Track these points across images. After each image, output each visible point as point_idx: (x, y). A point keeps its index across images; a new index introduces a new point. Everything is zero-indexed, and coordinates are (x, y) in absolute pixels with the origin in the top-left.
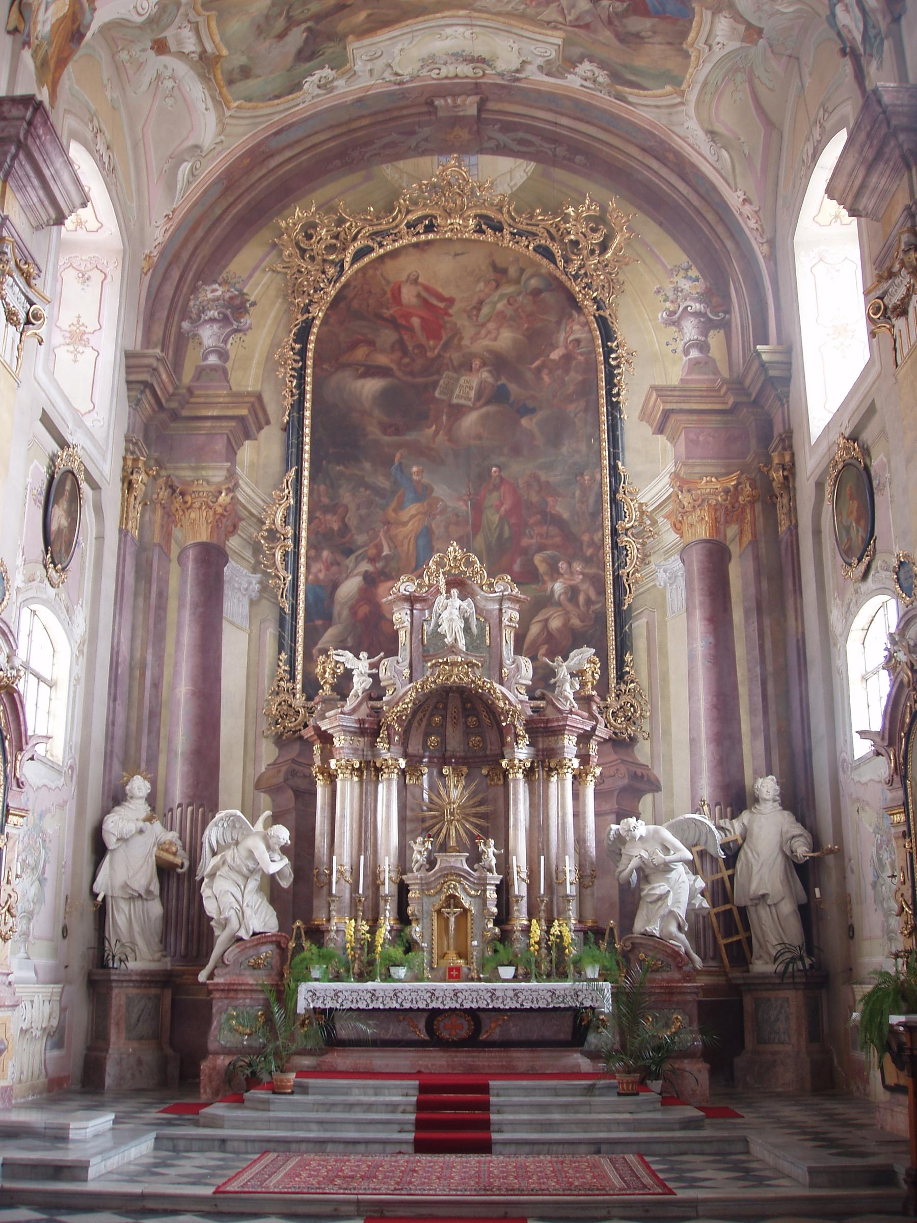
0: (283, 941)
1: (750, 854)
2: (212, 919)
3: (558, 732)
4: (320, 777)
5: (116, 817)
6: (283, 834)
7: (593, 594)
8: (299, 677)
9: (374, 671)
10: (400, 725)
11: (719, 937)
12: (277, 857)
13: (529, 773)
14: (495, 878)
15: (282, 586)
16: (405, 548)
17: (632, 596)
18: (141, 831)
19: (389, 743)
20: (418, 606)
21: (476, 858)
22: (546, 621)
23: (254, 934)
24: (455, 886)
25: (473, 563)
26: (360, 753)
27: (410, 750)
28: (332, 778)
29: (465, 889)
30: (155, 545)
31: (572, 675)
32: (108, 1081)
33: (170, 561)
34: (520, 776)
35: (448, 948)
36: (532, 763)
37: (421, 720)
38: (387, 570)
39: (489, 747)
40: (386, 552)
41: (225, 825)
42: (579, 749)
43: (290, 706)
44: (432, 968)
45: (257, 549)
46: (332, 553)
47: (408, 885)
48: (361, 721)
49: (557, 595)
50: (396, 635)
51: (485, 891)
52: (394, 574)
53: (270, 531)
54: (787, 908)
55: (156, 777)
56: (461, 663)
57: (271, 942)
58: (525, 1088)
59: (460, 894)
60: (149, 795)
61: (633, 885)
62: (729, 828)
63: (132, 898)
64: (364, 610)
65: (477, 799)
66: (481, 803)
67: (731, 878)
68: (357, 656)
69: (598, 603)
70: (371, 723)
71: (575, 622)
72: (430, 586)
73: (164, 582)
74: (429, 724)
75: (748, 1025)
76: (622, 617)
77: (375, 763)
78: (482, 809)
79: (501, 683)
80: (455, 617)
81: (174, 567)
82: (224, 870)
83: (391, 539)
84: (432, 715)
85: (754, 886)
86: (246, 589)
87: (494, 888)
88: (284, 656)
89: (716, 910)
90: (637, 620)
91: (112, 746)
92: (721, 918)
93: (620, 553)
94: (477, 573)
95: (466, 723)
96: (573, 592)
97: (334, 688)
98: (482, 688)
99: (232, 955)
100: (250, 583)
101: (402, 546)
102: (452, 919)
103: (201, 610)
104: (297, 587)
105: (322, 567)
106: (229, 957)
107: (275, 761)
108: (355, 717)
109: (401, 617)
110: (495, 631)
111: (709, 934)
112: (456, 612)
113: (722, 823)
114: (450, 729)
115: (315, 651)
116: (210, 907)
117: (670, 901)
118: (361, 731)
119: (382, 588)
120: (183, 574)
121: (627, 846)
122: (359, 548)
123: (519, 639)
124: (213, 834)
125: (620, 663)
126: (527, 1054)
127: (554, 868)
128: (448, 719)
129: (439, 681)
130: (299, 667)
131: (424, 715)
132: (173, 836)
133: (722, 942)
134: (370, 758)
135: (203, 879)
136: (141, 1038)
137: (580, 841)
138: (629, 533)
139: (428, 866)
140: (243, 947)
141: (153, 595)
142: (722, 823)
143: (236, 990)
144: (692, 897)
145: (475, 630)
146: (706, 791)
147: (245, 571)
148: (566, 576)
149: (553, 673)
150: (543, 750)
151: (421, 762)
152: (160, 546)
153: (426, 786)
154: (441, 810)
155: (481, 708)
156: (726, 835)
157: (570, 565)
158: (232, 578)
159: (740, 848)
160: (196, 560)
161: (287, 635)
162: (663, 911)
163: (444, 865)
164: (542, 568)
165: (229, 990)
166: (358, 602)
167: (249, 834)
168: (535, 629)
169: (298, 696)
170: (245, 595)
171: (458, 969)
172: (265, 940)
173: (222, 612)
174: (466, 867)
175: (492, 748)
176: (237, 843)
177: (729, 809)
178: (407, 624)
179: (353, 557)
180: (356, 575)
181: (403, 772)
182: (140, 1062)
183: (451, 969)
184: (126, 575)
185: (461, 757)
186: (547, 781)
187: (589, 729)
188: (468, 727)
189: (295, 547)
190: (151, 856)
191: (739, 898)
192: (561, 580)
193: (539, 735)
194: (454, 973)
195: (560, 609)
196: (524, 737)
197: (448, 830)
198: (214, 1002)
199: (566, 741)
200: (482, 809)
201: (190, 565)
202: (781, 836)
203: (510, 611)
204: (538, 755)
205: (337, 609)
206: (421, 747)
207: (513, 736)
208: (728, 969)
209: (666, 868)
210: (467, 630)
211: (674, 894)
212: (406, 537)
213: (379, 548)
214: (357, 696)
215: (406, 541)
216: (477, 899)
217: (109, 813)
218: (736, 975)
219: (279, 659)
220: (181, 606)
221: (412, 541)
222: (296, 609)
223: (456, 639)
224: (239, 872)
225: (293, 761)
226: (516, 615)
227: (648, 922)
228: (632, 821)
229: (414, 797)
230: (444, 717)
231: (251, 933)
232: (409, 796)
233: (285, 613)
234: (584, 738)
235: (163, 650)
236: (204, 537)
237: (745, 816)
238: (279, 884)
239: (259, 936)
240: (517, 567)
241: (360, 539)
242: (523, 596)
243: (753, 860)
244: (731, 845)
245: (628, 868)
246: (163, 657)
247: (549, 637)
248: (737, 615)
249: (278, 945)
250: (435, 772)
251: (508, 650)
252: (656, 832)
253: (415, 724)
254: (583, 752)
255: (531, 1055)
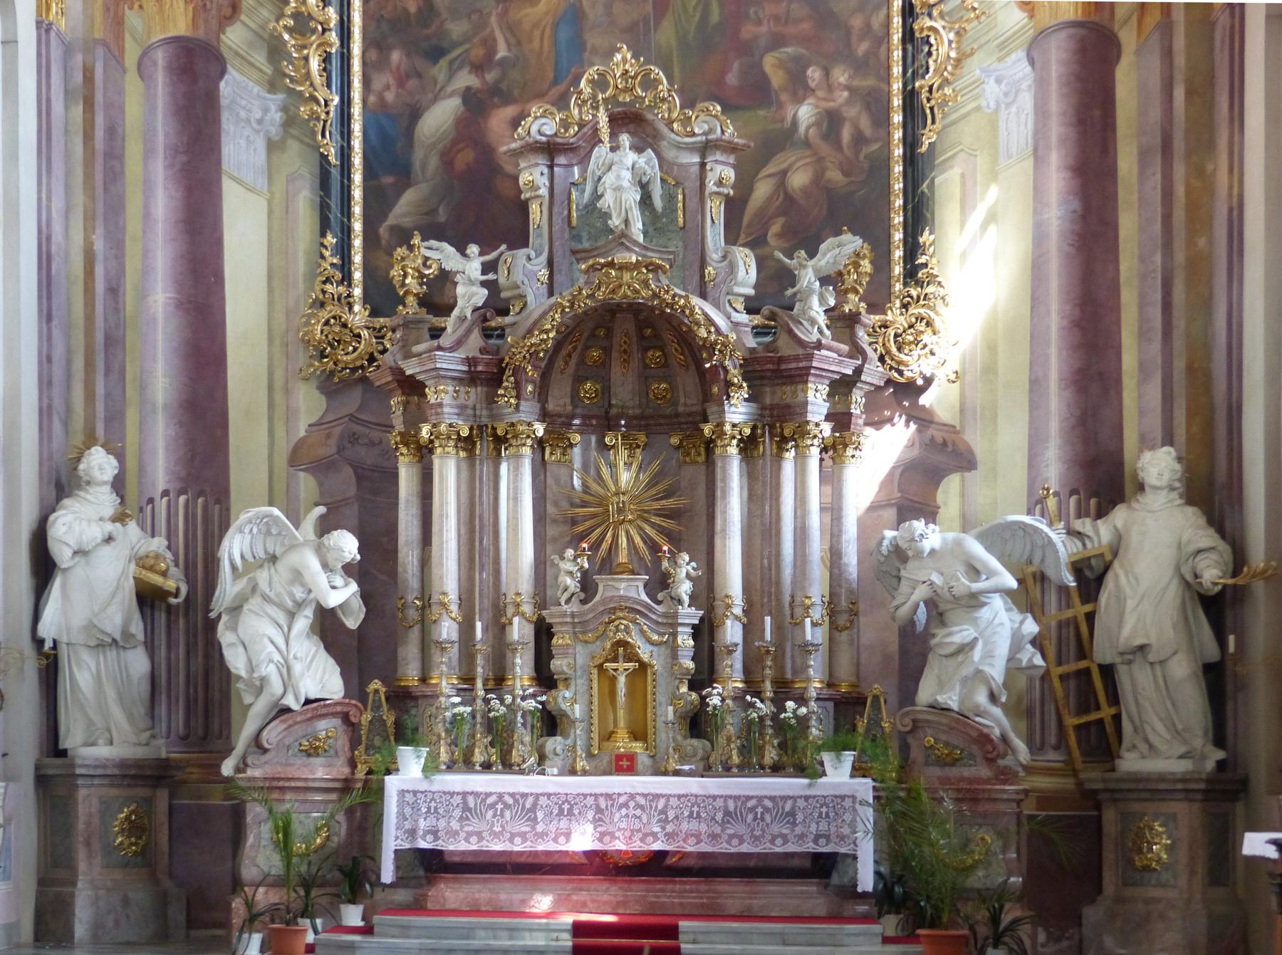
0: (352, 712)
1: (1123, 579)
2: (239, 678)
3: (800, 377)
4: (404, 450)
5: (70, 517)
6: (347, 545)
7: (865, 124)
8: (357, 275)
9: (491, 276)
10: (535, 368)
11: (1064, 713)
12: (339, 581)
13: (748, 446)
14: (690, 615)
15: (323, 116)
16: (536, 44)
17: (938, 126)
18: (109, 539)
19: (518, 397)
20: (561, 160)
21: (660, 583)
22: (783, 174)
23: (308, 702)
24: (627, 627)
25: (657, 82)
26: (470, 412)
27: (551, 406)
28: (424, 453)
29: (642, 632)
30: (96, 42)
31: (824, 281)
32: (81, 930)
33: (125, 72)
34: (733, 450)
35: (616, 725)
36: (754, 428)
37: (570, 355)
38: (504, 86)
39: (682, 400)
40: (502, 52)
41: (255, 530)
42: (833, 405)
43: (345, 325)
44: (590, 756)
45: (276, 51)
46: (408, 55)
47: (550, 626)
48: (470, 361)
49: (802, 129)
50: (524, 208)
51: (674, 635)
52: (516, 92)
53: (296, 15)
54: (1182, 669)
55: (123, 448)
56: (637, 265)
57: (334, 715)
58: (736, 933)
59: (636, 639)
60: (116, 477)
61: (920, 627)
62: (1091, 534)
63: (100, 646)
64: (465, 158)
65: (660, 487)
66: (668, 494)
67: (1090, 617)
68: (462, 251)
69: (877, 140)
70: (487, 364)
71: (834, 175)
72: (581, 125)
73: (116, 110)
74: (581, 362)
75: (1109, 856)
76: (917, 166)
77: (494, 429)
78: (669, 503)
79: (703, 296)
80: (626, 184)
81: (132, 84)
82: (254, 603)
83: (512, 29)
84: (587, 348)
85: (1126, 631)
86: (260, 122)
87: (689, 630)
88: (330, 240)
89: (1061, 670)
90: (945, 171)
91: (50, 398)
92: (1072, 684)
93: (916, 51)
94: (663, 100)
95: (643, 360)
96: (831, 121)
97: (424, 302)
98: (671, 306)
99: (274, 734)
100: (266, 111)
101: (530, 41)
102: (622, 680)
103: (184, 158)
104: (349, 116)
105: (392, 81)
106: (272, 735)
107: (322, 418)
108: (461, 354)
109: (533, 176)
110: (693, 204)
111: (1051, 709)
112: (627, 175)
113: (1078, 525)
114: (617, 371)
115: (383, 231)
116: (236, 661)
117: (977, 654)
118: (471, 378)
119: (499, 119)
120: (149, 98)
121: (910, 565)
122: (455, 45)
123: (734, 207)
124: (234, 546)
125: (912, 249)
126: (741, 888)
127: (787, 599)
128: (614, 354)
129: (600, 295)
130: (357, 259)
131: (575, 348)
132: (158, 544)
133: (1071, 721)
134: (485, 420)
135: (219, 616)
136: (126, 865)
137: (835, 556)
138: (935, 13)
139: (582, 596)
140: (291, 722)
141: (99, 134)
142: (1078, 525)
143: (282, 789)
144: (1016, 647)
145: (658, 203)
146: (1054, 471)
147: (256, 89)
148: (820, 93)
149: (789, 278)
150: (772, 407)
151: (569, 425)
152: (104, 43)
153: (577, 464)
154: (602, 502)
155: (668, 337)
156: (1084, 545)
157: (827, 73)
158: (233, 101)
159: (1107, 567)
160: (170, 68)
161: (334, 203)
162: (967, 671)
163: (609, 594)
164: (777, 79)
165: (271, 789)
166: (454, 143)
167: (293, 547)
168: (762, 190)
169: (357, 308)
170: (257, 132)
171: (631, 758)
172: (324, 711)
173: (219, 162)
174: (644, 597)
175: (688, 401)
176: (273, 559)
177: (1093, 501)
178: (544, 191)
179: (443, 63)
180: (451, 95)
181: (540, 444)
182: (126, 901)
183: (619, 758)
184: (53, 99)
185: (635, 417)
186: (779, 457)
187: (849, 372)
188: (646, 366)
189: (342, 45)
190: (127, 578)
191: (1103, 652)
192: (811, 100)
193: (766, 382)
194: (625, 763)
195: (808, 152)
196: (741, 387)
197: (615, 538)
198: (248, 805)
199: (811, 394)
200: (669, 503)
201: (161, 79)
202: (1179, 547)
203: (719, 168)
204: (762, 416)
205: (418, 155)
206: (568, 401)
207: (722, 384)
208: (1079, 765)
209: (974, 601)
210: (646, 201)
211: (985, 644)
212: (535, 25)
213: (491, 48)
214: (462, 319)
215: (537, 33)
216: (663, 648)
217: (54, 511)
218: (1093, 776)
219: (322, 245)
220: (148, 154)
221: (548, 31)
222: (349, 156)
223: (626, 222)
224: (280, 606)
225: (352, 417)
226: (730, 174)
227: (941, 686)
228: (919, 525)
229: (557, 481)
230: (607, 351)
231: (303, 701)
232: (550, 481)
233: (329, 164)
234: (842, 386)
235: (123, 230)
236: (181, 26)
237: (1119, 515)
238: (343, 625)
239: (315, 705)
240: (732, 79)
241: (457, 29)
242: (741, 141)
243: (1128, 590)
244: (1093, 562)
245: (911, 599)
246: (123, 241)
247: (787, 202)
248: (1127, 161)
249: (346, 718)
250: (593, 439)
251: (715, 236)
252: (958, 543)
253: (560, 363)
254: (840, 408)
255: (747, 888)
